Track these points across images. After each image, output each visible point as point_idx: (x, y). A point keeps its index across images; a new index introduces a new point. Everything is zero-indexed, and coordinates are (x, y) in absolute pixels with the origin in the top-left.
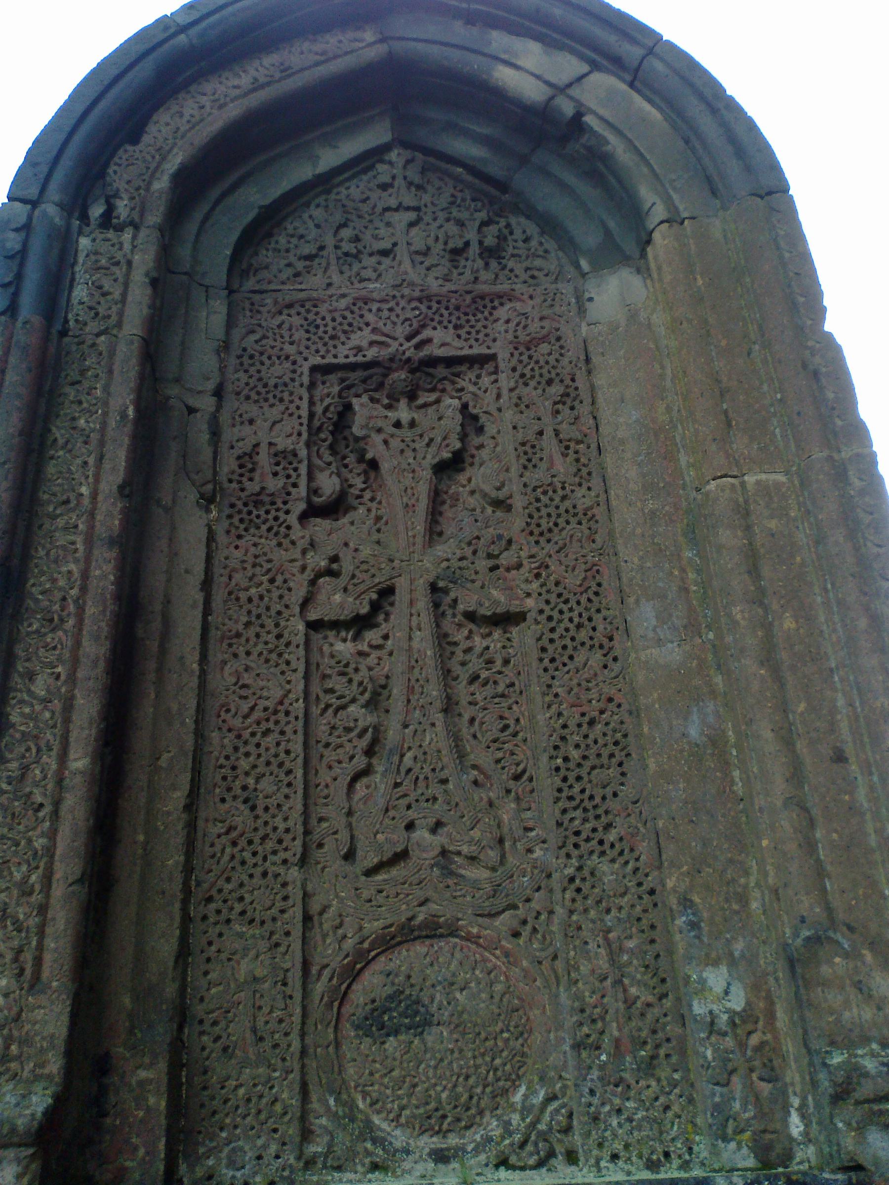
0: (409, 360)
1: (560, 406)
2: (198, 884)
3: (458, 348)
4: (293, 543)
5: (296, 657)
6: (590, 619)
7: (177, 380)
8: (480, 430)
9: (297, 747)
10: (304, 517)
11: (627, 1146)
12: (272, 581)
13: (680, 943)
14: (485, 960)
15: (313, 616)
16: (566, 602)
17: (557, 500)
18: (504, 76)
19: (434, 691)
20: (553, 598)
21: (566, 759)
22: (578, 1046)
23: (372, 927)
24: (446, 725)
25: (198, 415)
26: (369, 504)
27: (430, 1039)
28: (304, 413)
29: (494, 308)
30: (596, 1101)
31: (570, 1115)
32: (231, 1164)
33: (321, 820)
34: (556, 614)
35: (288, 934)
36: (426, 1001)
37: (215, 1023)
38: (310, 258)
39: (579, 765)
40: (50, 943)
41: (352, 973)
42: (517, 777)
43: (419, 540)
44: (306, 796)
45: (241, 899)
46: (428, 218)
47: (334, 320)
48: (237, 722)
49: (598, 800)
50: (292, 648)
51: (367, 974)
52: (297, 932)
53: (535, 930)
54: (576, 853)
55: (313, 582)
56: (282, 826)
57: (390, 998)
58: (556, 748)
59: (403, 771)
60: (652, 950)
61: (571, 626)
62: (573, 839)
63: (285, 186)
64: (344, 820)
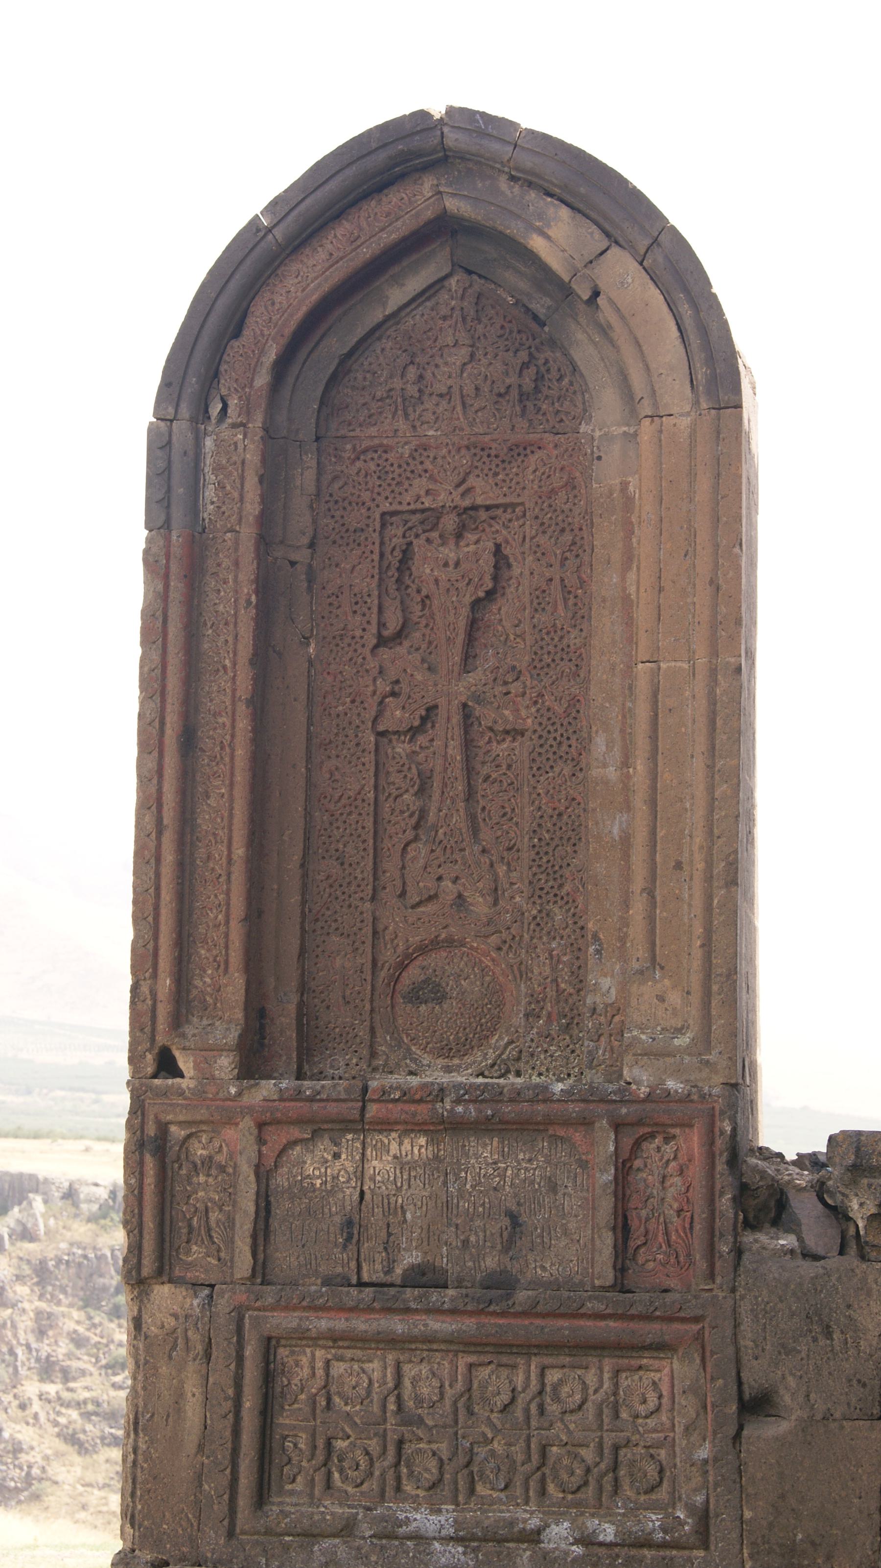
0: (456, 507)
1: (568, 554)
2: (310, 911)
3: (493, 497)
4: (367, 671)
5: (369, 759)
6: (568, 738)
7: (282, 542)
8: (509, 566)
9: (369, 824)
10: (376, 647)
11: (548, 1070)
12: (353, 701)
13: (591, 963)
14: (481, 961)
15: (381, 728)
16: (553, 724)
17: (557, 639)
18: (537, 243)
19: (460, 787)
20: (544, 721)
21: (540, 840)
22: (527, 1016)
23: (415, 940)
24: (467, 809)
25: (298, 566)
26: (424, 630)
27: (445, 1006)
28: (376, 557)
29: (526, 455)
30: (534, 1045)
31: (521, 1052)
32: (332, 1067)
33: (384, 872)
34: (545, 734)
35: (363, 943)
36: (444, 985)
37: (322, 992)
38: (381, 400)
39: (548, 844)
40: (232, 954)
41: (402, 966)
42: (510, 849)
43: (456, 669)
44: (375, 857)
45: (336, 921)
46: (479, 354)
47: (400, 466)
48: (332, 807)
49: (557, 868)
50: (366, 754)
51: (411, 967)
52: (369, 942)
53: (510, 946)
54: (539, 901)
55: (381, 703)
56: (360, 876)
57: (424, 982)
58: (534, 831)
59: (437, 841)
60: (577, 964)
61: (554, 743)
62: (538, 892)
63: (360, 332)
64: (399, 873)
